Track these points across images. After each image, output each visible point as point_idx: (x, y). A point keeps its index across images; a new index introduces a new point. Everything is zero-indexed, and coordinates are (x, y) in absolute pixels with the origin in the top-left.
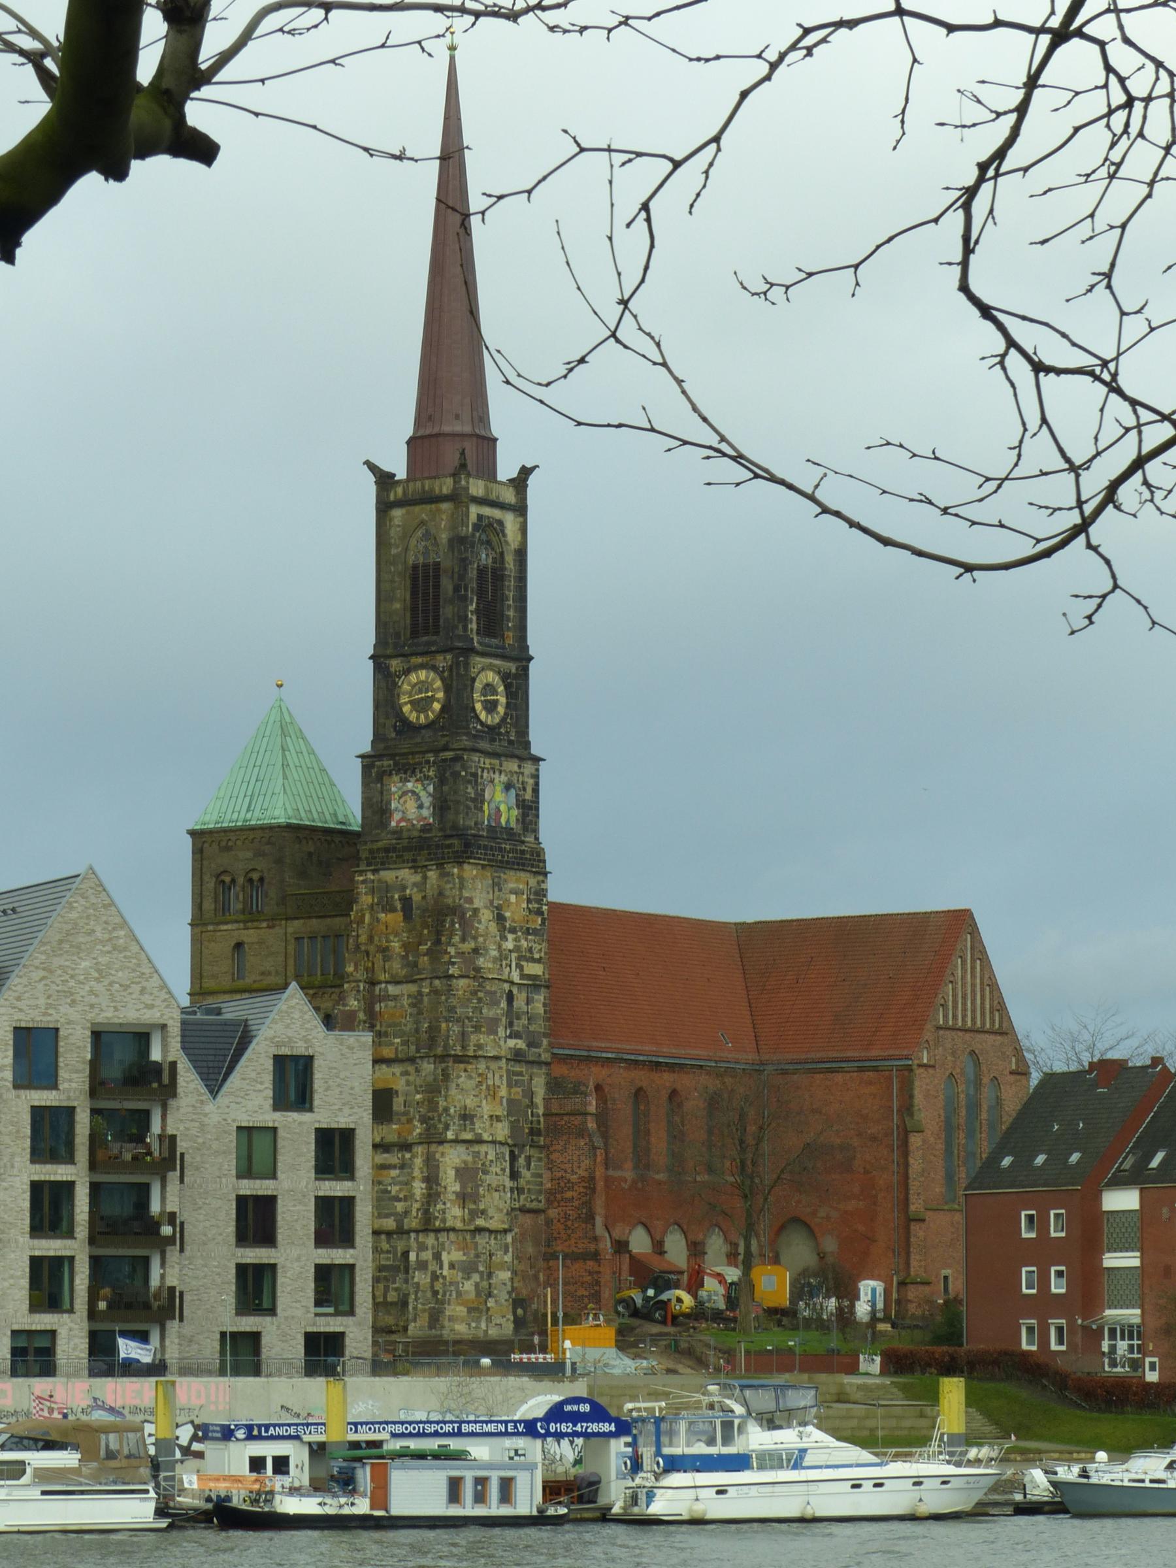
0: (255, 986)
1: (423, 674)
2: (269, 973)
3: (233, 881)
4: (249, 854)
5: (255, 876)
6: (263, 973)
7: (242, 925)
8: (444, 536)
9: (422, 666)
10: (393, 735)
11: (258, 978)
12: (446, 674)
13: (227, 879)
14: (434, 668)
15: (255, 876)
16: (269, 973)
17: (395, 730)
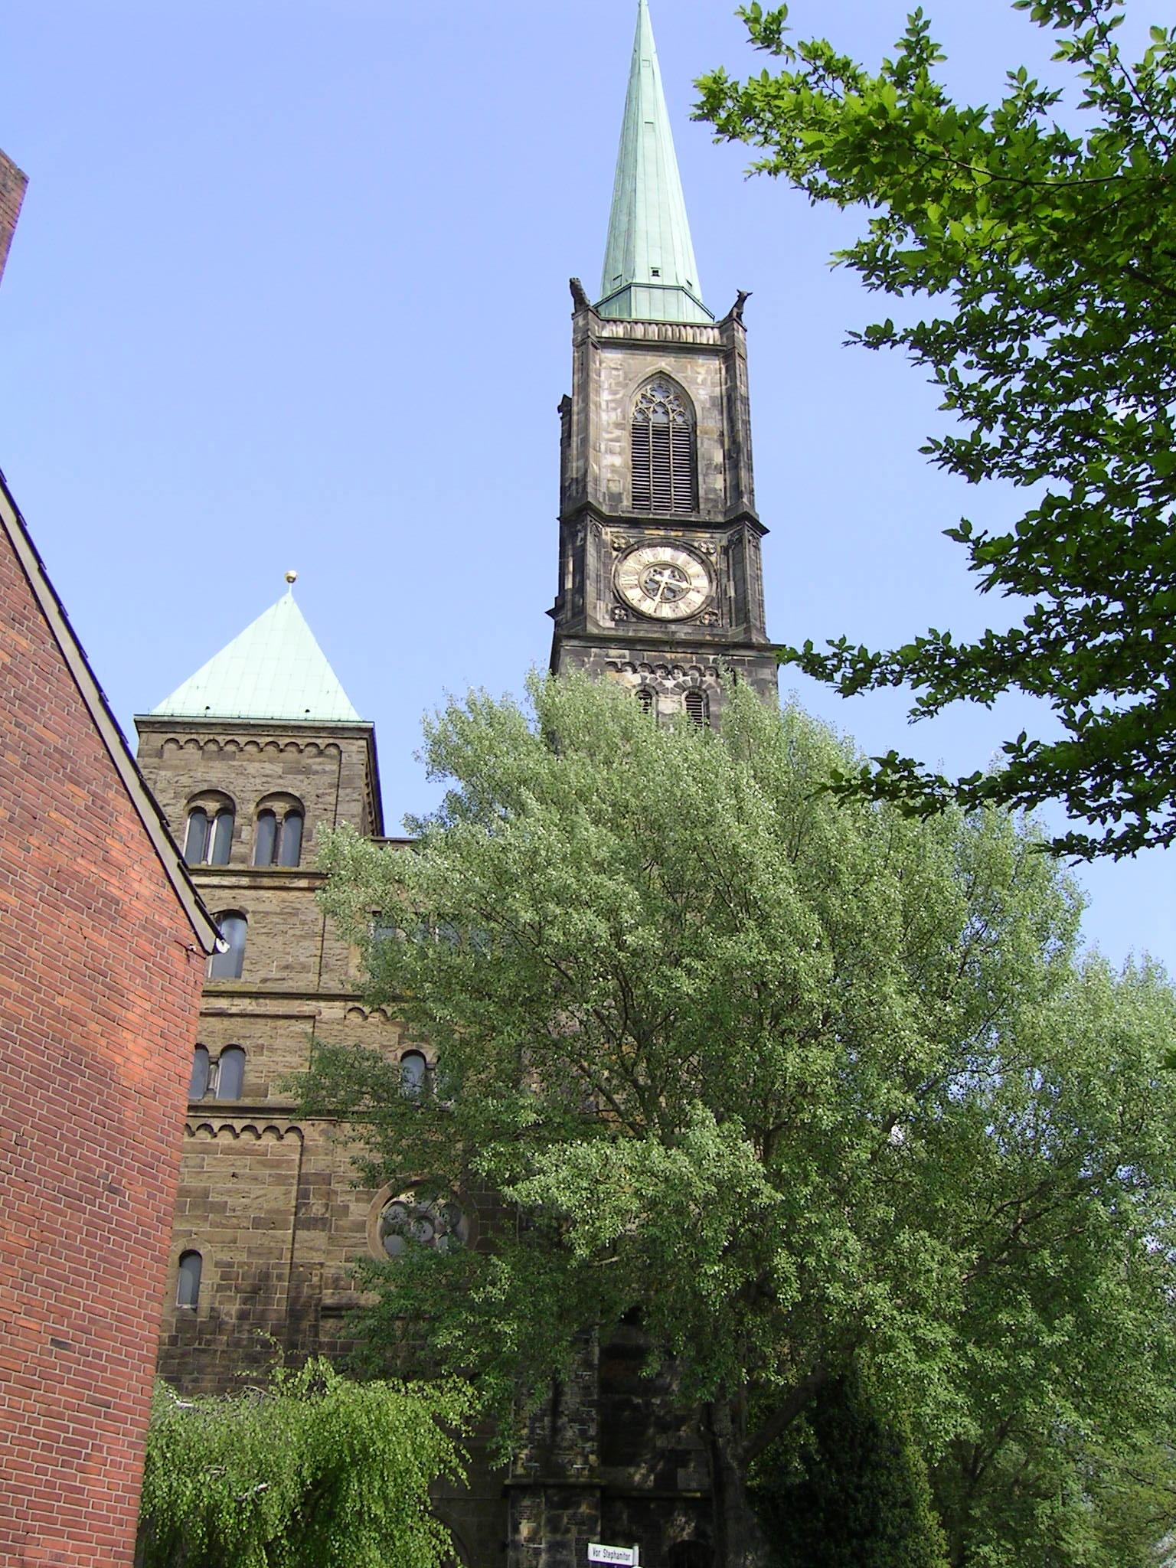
0: (270, 987)
1: (666, 554)
2: (305, 968)
3: (228, 810)
4: (278, 769)
5: (280, 807)
6: (287, 967)
7: (245, 881)
8: (701, 392)
9: (666, 543)
10: (612, 624)
11: (274, 975)
12: (713, 558)
13: (212, 806)
14: (691, 550)
15: (280, 807)
16: (305, 968)
17: (613, 619)
